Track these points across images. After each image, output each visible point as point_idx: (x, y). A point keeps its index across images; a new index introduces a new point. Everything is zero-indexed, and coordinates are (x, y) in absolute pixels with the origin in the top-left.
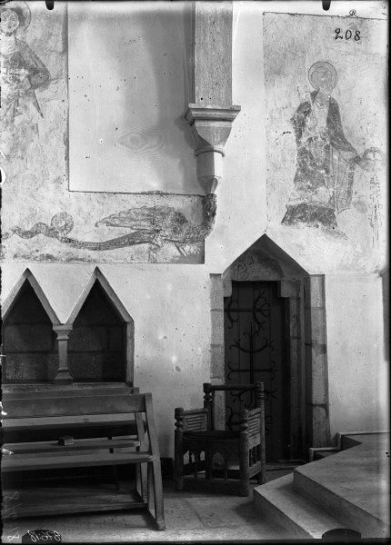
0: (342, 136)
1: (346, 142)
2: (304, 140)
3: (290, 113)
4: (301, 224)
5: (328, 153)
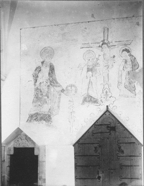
0: (56, 81)
1: (57, 83)
2: (38, 83)
3: (32, 72)
4: (35, 122)
5: (48, 89)
